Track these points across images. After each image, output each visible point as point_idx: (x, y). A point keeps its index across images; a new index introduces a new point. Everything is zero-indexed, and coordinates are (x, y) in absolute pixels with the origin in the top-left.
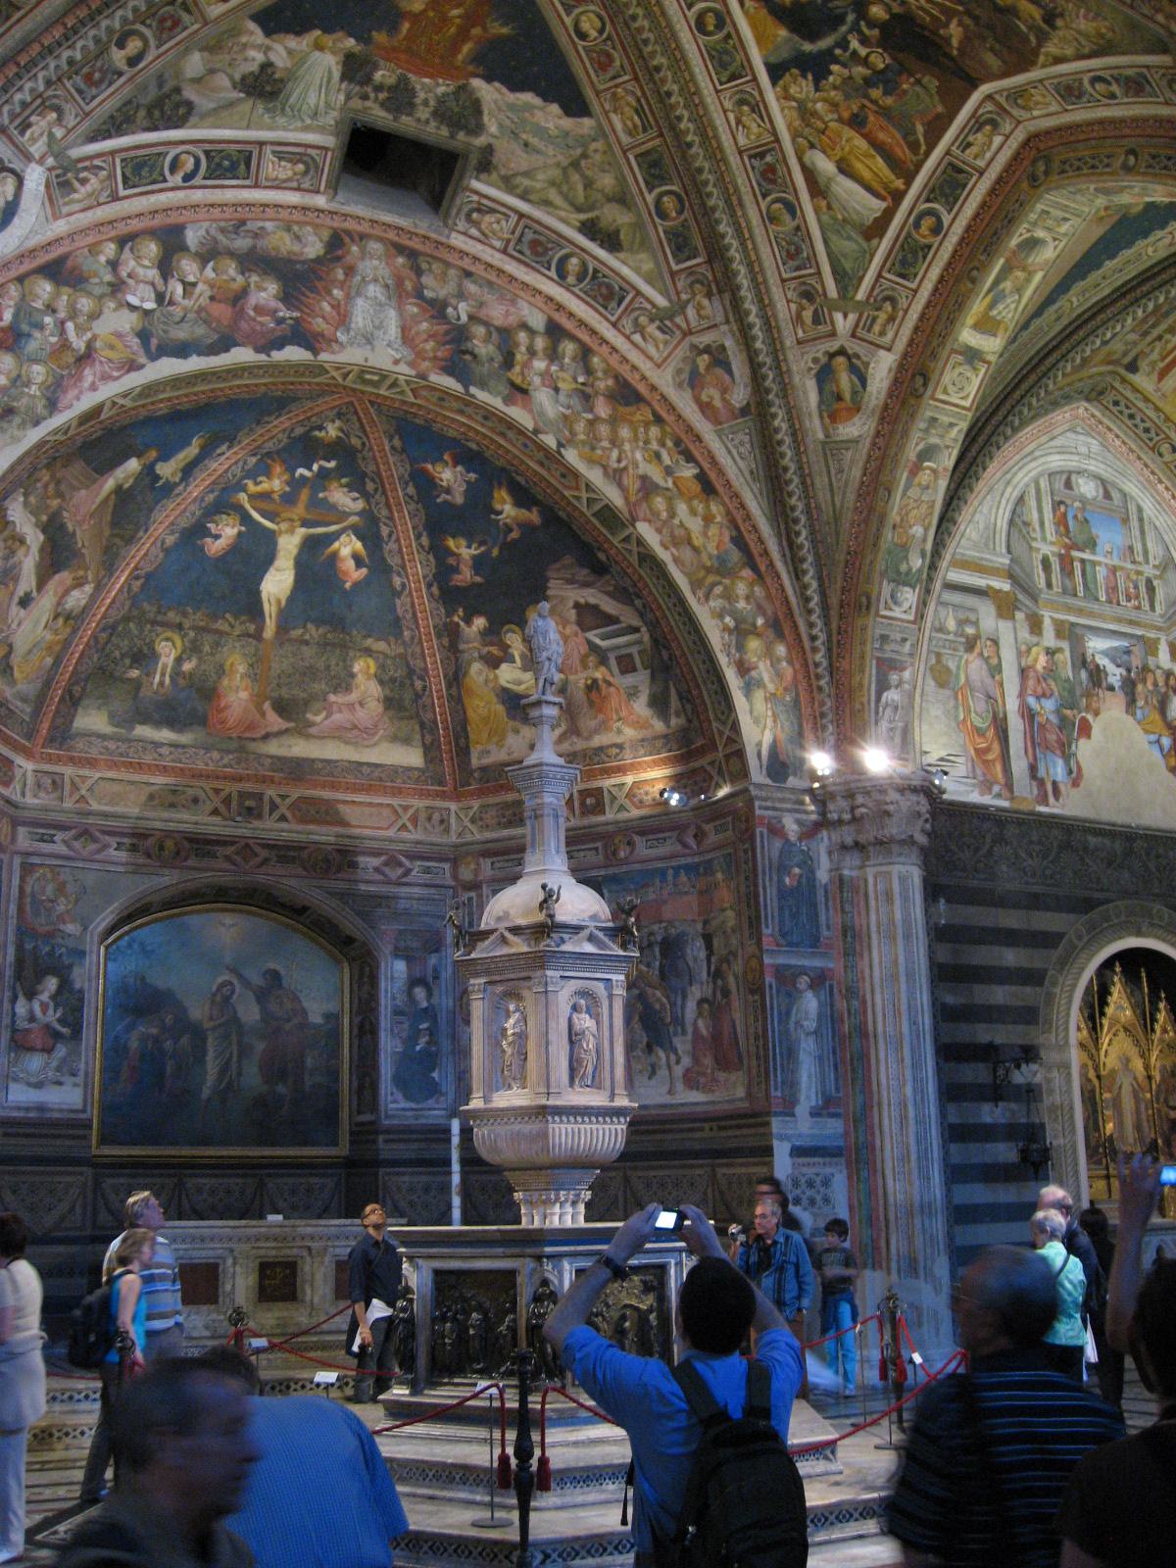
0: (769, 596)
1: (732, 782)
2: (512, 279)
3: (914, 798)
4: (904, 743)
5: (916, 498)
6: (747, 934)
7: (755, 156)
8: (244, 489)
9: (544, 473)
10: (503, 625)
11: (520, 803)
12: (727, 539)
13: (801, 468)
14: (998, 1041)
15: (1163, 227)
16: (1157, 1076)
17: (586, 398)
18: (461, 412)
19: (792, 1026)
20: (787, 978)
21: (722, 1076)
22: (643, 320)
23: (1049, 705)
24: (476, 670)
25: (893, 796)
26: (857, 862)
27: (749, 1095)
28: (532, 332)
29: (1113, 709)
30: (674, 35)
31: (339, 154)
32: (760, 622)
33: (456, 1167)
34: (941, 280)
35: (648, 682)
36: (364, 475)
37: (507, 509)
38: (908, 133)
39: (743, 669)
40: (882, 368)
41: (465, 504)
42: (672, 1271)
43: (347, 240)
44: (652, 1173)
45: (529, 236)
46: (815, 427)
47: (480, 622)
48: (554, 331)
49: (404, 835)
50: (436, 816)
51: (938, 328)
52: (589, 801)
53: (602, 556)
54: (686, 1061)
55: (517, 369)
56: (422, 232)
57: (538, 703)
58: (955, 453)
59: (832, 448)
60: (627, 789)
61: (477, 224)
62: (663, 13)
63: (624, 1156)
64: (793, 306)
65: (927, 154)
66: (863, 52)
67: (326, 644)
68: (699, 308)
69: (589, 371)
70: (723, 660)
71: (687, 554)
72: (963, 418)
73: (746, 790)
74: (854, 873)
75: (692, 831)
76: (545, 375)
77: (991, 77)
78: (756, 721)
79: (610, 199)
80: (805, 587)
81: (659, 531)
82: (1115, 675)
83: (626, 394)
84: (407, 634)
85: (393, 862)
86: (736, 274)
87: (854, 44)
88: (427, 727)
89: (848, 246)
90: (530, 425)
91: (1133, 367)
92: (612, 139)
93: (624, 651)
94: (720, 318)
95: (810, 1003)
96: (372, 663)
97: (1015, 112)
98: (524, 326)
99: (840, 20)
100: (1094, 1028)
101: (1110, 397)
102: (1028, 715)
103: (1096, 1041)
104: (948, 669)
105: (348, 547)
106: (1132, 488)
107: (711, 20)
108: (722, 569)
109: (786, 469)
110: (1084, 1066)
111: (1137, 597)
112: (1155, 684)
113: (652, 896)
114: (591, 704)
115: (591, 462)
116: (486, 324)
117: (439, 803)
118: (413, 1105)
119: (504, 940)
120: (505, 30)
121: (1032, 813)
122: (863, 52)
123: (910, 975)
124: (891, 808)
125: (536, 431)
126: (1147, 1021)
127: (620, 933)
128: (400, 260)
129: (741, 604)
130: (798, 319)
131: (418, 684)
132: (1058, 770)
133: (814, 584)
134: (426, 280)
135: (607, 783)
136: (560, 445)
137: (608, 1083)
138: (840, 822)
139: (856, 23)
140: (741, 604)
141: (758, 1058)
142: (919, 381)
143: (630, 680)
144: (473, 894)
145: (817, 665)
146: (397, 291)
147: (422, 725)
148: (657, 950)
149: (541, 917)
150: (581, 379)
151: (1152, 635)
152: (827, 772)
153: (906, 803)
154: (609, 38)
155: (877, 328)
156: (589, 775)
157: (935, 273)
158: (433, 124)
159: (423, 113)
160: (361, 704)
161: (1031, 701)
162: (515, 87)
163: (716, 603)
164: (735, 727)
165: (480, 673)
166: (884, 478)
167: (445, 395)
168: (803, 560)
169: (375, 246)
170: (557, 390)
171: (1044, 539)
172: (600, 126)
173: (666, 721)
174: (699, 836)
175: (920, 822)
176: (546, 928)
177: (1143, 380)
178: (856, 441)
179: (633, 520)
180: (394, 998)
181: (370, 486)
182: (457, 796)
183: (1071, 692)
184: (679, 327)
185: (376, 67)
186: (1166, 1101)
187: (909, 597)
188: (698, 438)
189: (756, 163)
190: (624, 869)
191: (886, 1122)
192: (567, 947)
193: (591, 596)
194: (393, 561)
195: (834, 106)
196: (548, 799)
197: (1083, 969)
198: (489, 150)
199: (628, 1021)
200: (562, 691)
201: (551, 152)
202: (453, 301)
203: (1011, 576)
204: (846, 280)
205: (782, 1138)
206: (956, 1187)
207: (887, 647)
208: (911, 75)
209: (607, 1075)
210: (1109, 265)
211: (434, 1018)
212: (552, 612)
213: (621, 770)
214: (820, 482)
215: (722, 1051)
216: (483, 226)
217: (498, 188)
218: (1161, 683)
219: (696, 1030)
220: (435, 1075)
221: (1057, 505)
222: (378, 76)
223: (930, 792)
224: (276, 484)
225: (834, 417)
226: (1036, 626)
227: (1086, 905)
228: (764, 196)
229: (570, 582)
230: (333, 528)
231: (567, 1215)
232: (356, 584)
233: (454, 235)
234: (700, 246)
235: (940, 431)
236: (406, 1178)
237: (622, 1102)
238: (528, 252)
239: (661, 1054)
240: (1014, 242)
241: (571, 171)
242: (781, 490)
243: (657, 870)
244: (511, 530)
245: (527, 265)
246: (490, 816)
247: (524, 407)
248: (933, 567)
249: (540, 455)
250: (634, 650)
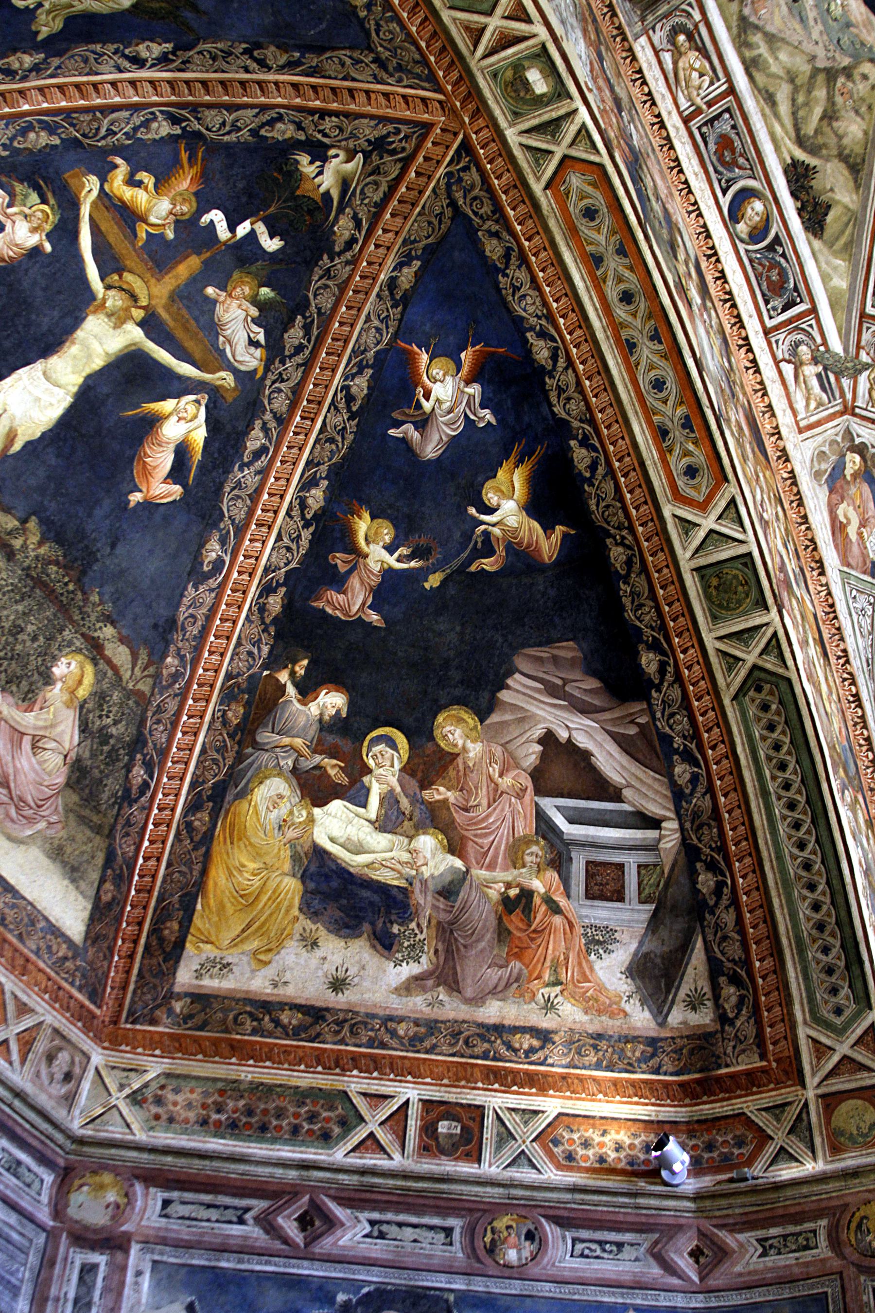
8: (104, 173)
35: (640, 928)
36: (303, 306)
45: (724, 126)
47: (332, 701)
50: (63, 1057)
52: (443, 1127)
53: (649, 662)
60: (542, 1123)
67: (39, 583)
79: (843, 157)
88: (116, 869)
105: (183, 423)
114: (502, 933)
117: (75, 1033)
131: (138, 773)
143: (602, 913)
144: (100, 1259)
160: (35, 747)
173: (660, 1013)
174: (710, 1255)
181: (294, 335)
182: (111, 1037)
194: (232, 508)
216: (681, 64)
217: (729, 28)
224: (160, 208)
229: (553, 691)
230: (186, 369)
232: (149, 506)
233: (643, 40)
238: (712, 147)
241: (821, 78)
246: (179, 1101)
250: (631, 861)
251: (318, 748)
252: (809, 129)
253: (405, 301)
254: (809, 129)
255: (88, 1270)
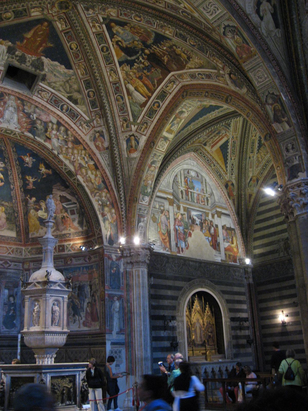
0: (111, 196)
1: (99, 245)
2: (49, 109)
3: (146, 251)
4: (144, 235)
5: (150, 173)
6: (101, 285)
7: (114, 84)
9: (53, 160)
10: (40, 200)
11: (42, 248)
12: (101, 181)
13: (121, 164)
14: (166, 314)
15: (214, 111)
16: (206, 324)
17: (66, 142)
18: (32, 143)
19: (112, 310)
20: (111, 297)
21: (93, 323)
22: (82, 123)
23: (181, 228)
24: (32, 212)
25: (141, 250)
26: (131, 267)
27: (100, 328)
28: (53, 123)
29: (197, 230)
30: (95, 52)
31: (4, 72)
32: (108, 203)
33: (19, 347)
34: (159, 119)
36: (5, 157)
37: (43, 170)
38: (153, 82)
39: (103, 215)
40: (143, 140)
41: (32, 167)
42: (77, 377)
43: (5, 95)
44: (74, 349)
45: (54, 98)
46: (125, 154)
47: (34, 199)
48: (59, 124)
49: (10, 255)
50: (19, 251)
51: (158, 131)
53: (67, 183)
54: (84, 319)
55: (48, 133)
56: (25, 95)
57: (48, 222)
58: (160, 163)
59: (129, 159)
61: (40, 94)
62: (93, 46)
63: (66, 345)
64: (121, 123)
65: (157, 88)
66: (143, 61)
68: (97, 121)
69: (67, 135)
70: (98, 213)
71: (90, 184)
72: (162, 154)
73: (102, 247)
74: (130, 270)
75: (88, 257)
76: (56, 135)
77: (175, 71)
78: (106, 229)
79: (75, 91)
80: (120, 195)
81: (83, 178)
82: (198, 221)
83: (77, 142)
84: (14, 201)
85: (6, 262)
86: (107, 113)
87: (141, 59)
88: (18, 226)
89: (136, 109)
90: (51, 148)
91: (205, 145)
92: (78, 76)
93: (73, 209)
94: (102, 124)
95: (117, 304)
96: (3, 208)
97: (180, 80)
98: (51, 122)
99: (138, 52)
100: (190, 311)
101: (199, 152)
102: (176, 230)
103: (191, 315)
104: (156, 218)
106: (204, 174)
107: (105, 49)
108: (99, 189)
109: (117, 164)
110: (187, 321)
111: (204, 202)
112: (208, 224)
113: (76, 274)
114: (62, 222)
115: (66, 158)
116: (41, 120)
117: (19, 247)
118: (8, 330)
119: (35, 285)
120: (52, 45)
121: (176, 256)
122: (143, 61)
123: (144, 297)
124: (140, 253)
125: (52, 150)
126: (203, 310)
127: (67, 284)
128: (19, 102)
129: (104, 198)
130: (122, 126)
131: (16, 215)
132: (183, 245)
133: (123, 194)
134: (25, 107)
135: (66, 244)
136: (58, 153)
137: (62, 325)
138: (127, 256)
139: (142, 53)
140: (104, 198)
141: (103, 318)
142: (152, 144)
143: (73, 216)
144: (28, 272)
145: (122, 215)
146: (17, 110)
147: (16, 226)
148: (77, 289)
149: (46, 279)
150: (65, 137)
151: (207, 211)
152: (124, 243)
153: (144, 252)
154: (79, 50)
155: (142, 130)
156: (61, 241)
157: (158, 117)
158: (31, 67)
159: (28, 64)
161: (177, 227)
162: (53, 60)
163: (97, 198)
164: (100, 230)
165: (33, 212)
166: (142, 168)
167: (28, 138)
168: (120, 188)
169: (12, 97)
170: (58, 139)
171: (182, 186)
172: (75, 72)
175: (147, 257)
176: (47, 282)
177: (208, 148)
178: (135, 158)
179: (76, 175)
180: (4, 300)
181: (6, 161)
182: (25, 245)
183: (187, 225)
184: (91, 125)
185: (16, 51)
186: (208, 330)
187: (147, 199)
188: (95, 154)
189: (114, 86)
190: (69, 267)
191: (136, 336)
192: (52, 288)
193: (64, 194)
194: (11, 181)
195: (135, 73)
196: (49, 247)
197: (187, 296)
198: (45, 75)
199: (68, 307)
200: (55, 218)
201: (61, 77)
202: (32, 114)
203: (173, 195)
204: (135, 117)
205: (108, 340)
206: (154, 353)
207: (141, 212)
208: (154, 68)
209: (62, 323)
210: (200, 119)
211: (15, 306)
212: (53, 197)
213: (70, 240)
214: (126, 168)
215: (93, 316)
216: (42, 95)
218: (209, 224)
219: (87, 310)
220: (15, 322)
221: (185, 177)
222: (17, 53)
223: (150, 249)
225: (130, 152)
226: (179, 208)
227: (189, 280)
228: (116, 94)
229: (59, 190)
231: (49, 361)
234: (98, 105)
235: (157, 157)
236: (5, 351)
237: (66, 330)
238: (53, 103)
239: (77, 317)
240: (177, 111)
242: (115, 169)
243: (78, 267)
244: (44, 175)
245: (52, 106)
246: (33, 251)
247: (49, 143)
248: (153, 191)
249: (53, 156)
250: (75, 209)
251: (35, 205)
252: (68, 90)
253: (16, 152)
254: (68, 90)
255: (27, 274)
